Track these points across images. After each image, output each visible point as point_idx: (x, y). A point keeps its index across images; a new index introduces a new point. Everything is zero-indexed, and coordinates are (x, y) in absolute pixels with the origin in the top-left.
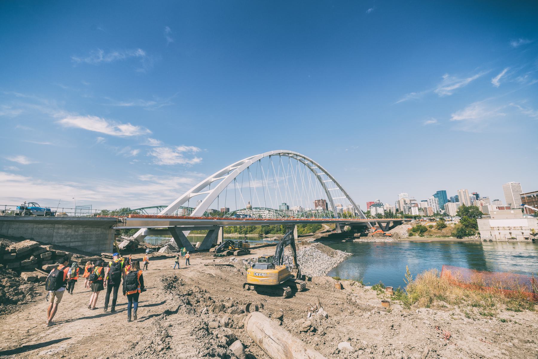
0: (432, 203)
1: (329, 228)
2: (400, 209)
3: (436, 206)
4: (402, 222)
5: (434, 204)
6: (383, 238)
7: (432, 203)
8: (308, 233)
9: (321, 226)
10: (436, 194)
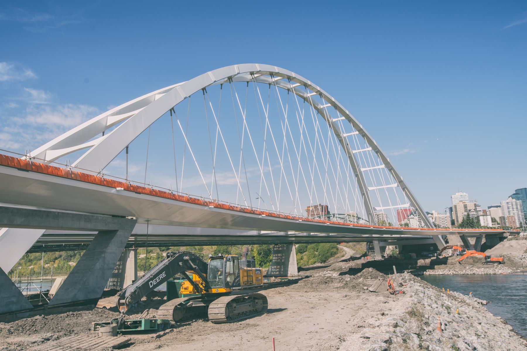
0: (511, 209)
1: (354, 252)
2: (458, 221)
3: (518, 215)
4: (505, 235)
5: (515, 211)
6: (485, 266)
7: (511, 209)
8: (312, 264)
9: (337, 249)
10: (514, 194)
